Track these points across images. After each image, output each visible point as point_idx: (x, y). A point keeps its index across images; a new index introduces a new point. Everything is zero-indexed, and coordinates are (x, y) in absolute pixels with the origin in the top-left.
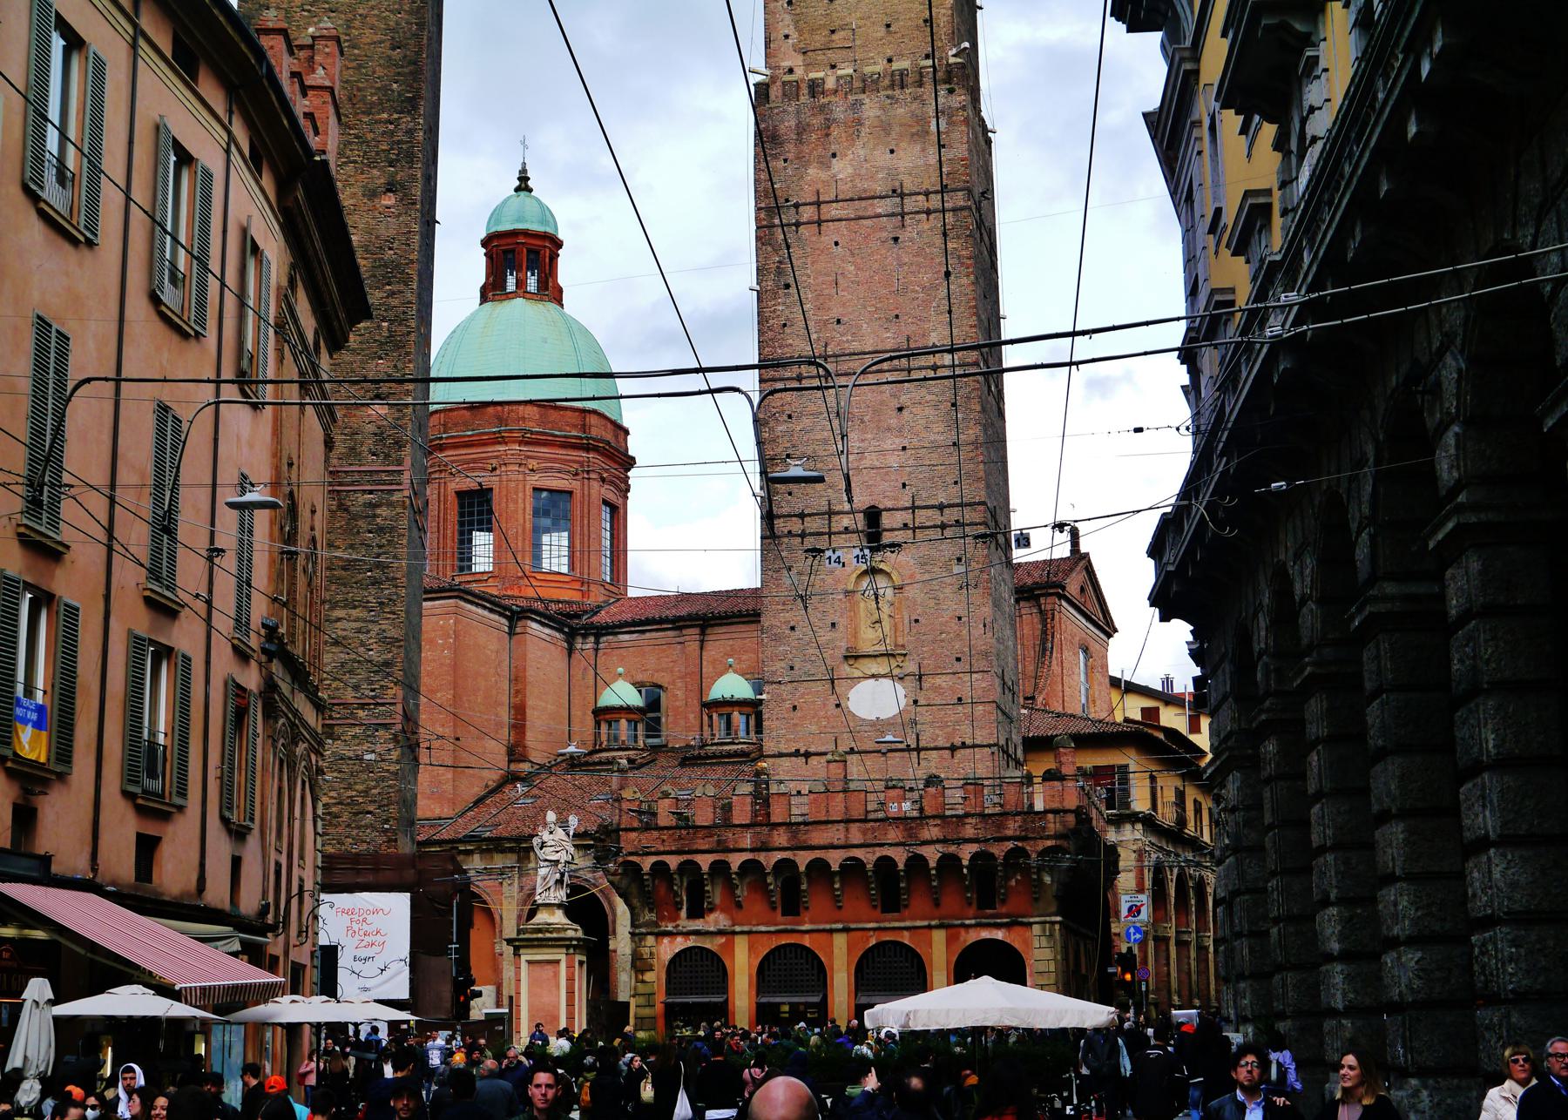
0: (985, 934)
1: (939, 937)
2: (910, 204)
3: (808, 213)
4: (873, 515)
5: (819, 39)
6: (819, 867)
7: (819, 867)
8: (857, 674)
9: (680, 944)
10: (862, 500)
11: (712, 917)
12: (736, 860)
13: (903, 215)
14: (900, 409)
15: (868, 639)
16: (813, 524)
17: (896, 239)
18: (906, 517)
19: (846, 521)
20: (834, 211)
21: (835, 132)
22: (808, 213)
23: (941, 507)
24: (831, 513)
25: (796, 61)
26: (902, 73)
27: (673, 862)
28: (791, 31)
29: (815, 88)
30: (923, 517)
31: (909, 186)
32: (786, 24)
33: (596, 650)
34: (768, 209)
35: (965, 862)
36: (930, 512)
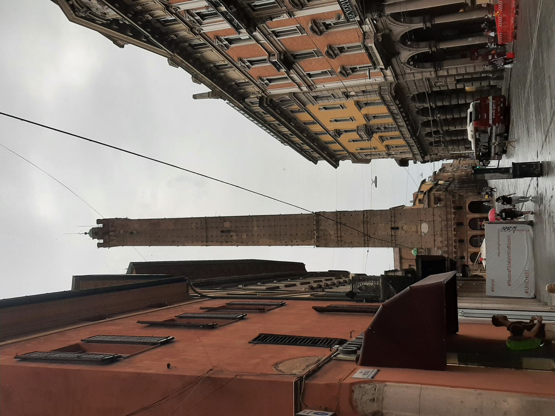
0: (467, 208)
1: (468, 216)
3: (339, 239)
4: (392, 228)
6: (455, 235)
7: (455, 235)
10: (389, 231)
12: (454, 250)
15: (414, 229)
16: (393, 239)
18: (393, 223)
19: (393, 233)
20: (339, 234)
23: (391, 217)
24: (392, 235)
25: (313, 240)
29: (317, 237)
30: (393, 220)
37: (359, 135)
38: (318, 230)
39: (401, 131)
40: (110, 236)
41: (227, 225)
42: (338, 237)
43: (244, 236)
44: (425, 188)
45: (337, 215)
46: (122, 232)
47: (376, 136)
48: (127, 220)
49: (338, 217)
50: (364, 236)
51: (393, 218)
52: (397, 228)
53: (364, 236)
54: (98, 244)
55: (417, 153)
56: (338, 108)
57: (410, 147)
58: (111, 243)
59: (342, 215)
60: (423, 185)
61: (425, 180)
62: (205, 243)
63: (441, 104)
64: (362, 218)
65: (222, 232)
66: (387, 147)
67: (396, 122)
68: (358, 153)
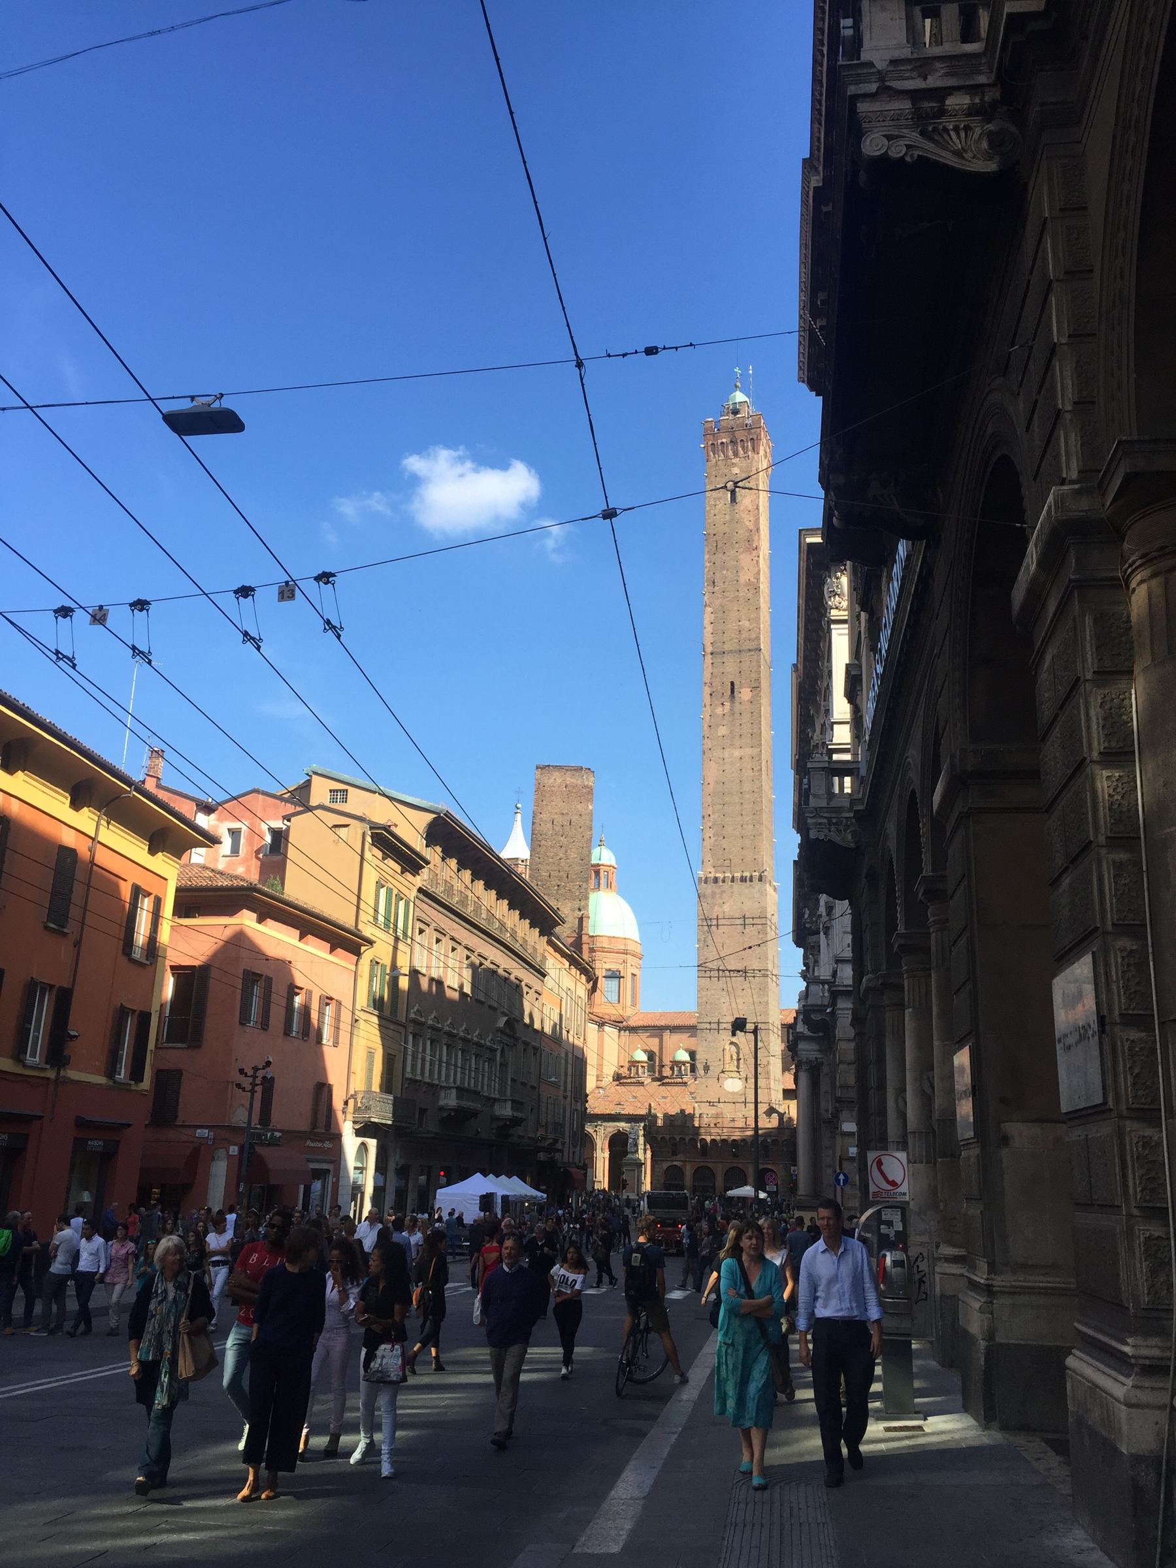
3: (714, 922)
5: (720, 863)
9: (669, 1164)
19: (724, 1026)
25: (712, 870)
27: (667, 1137)
32: (708, 857)
41: (745, 694)
43: (722, 731)
49: (756, 921)
62: (709, 649)
65: (732, 684)
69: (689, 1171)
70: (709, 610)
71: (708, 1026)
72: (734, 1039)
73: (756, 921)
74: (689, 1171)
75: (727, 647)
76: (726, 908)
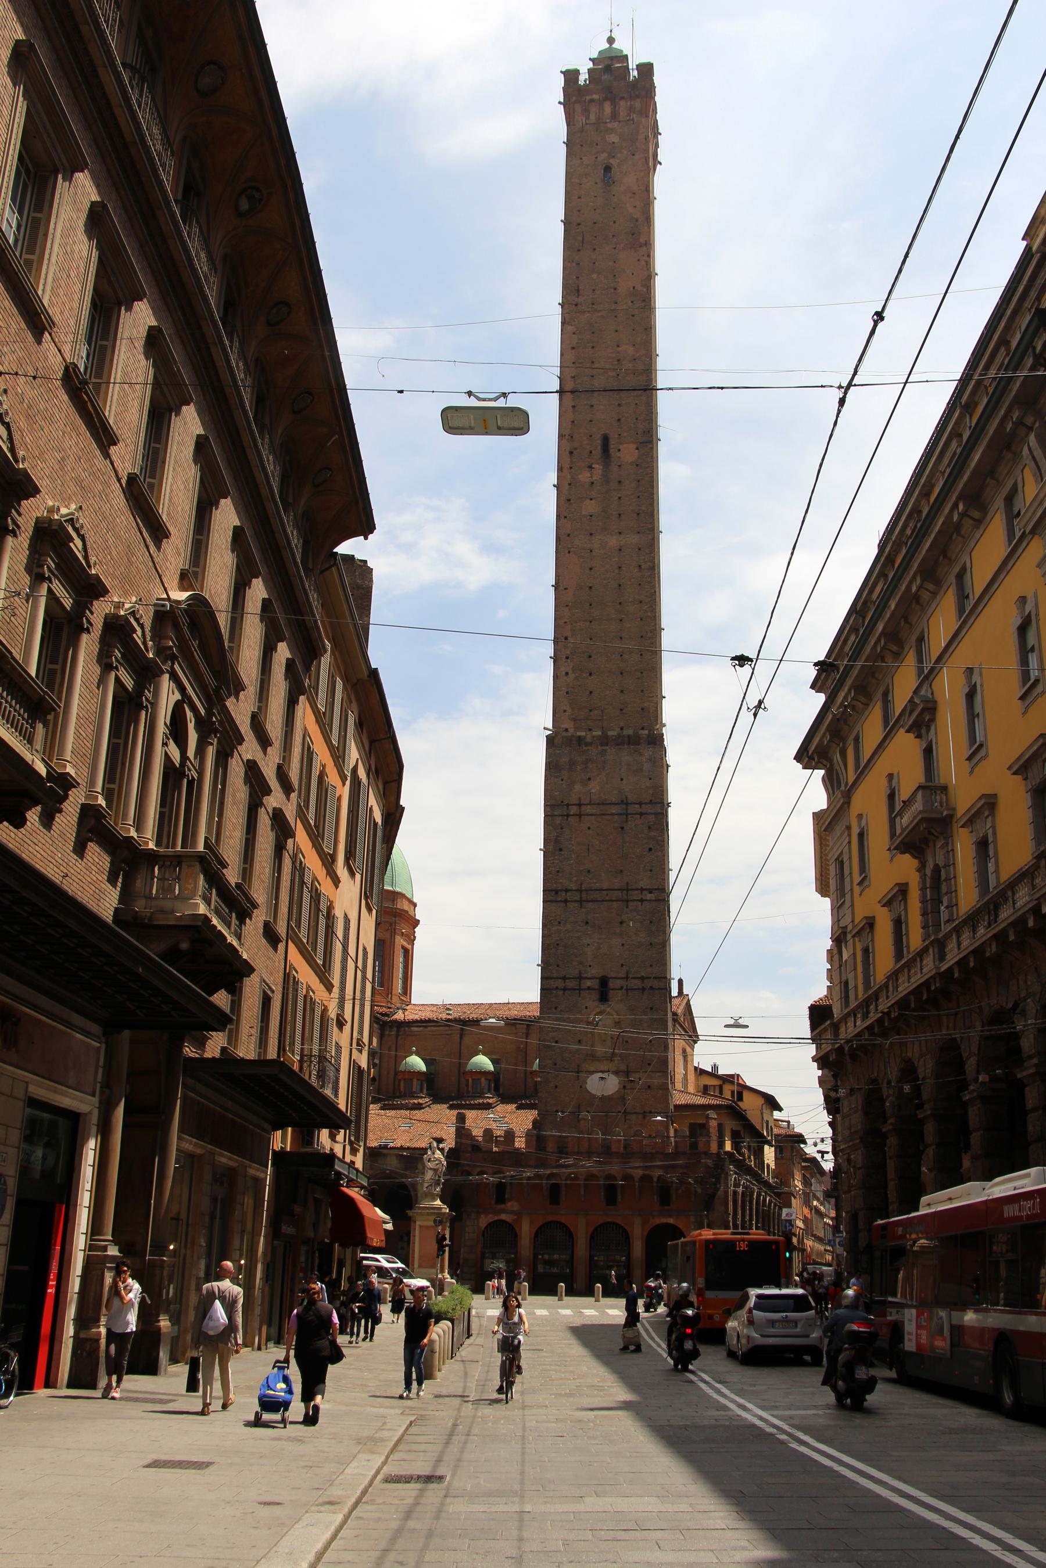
0: (664, 1220)
2: (631, 810)
3: (574, 810)
4: (604, 982)
8: (592, 1069)
10: (595, 971)
11: (509, 1204)
13: (627, 815)
14: (621, 923)
16: (570, 984)
17: (622, 828)
19: (589, 983)
20: (588, 809)
21: (590, 765)
22: (574, 810)
23: (642, 978)
24: (580, 978)
25: (568, 724)
26: (629, 736)
28: (567, 708)
29: (580, 739)
31: (631, 799)
33: (397, 1036)
34: (551, 806)
35: (655, 1179)
36: (636, 981)
37: (914, 794)
38: (604, 741)
39: (921, 954)
40: (600, 103)
41: (627, 453)
42: (580, 805)
43: (590, 507)
44: (749, 1104)
45: (651, 802)
46: (613, 138)
47: (906, 868)
48: (649, 162)
49: (645, 809)
50: (580, 891)
51: (638, 983)
52: (604, 998)
53: (580, 891)
54: (576, 72)
55: (842, 1035)
56: (1025, 675)
57: (865, 1006)
58: (578, 108)
59: (652, 818)
60: (762, 1101)
61: (780, 1109)
62: (569, 387)
63: (1030, 1104)
64: (642, 884)
65: (606, 440)
66: (870, 924)
67: (958, 930)
68: (849, 828)
69: (526, 1230)
70: (570, 328)
71: (560, 984)
72: (603, 1007)
73: (645, 809)
74: (526, 1230)
75: (597, 384)
76: (594, 787)
